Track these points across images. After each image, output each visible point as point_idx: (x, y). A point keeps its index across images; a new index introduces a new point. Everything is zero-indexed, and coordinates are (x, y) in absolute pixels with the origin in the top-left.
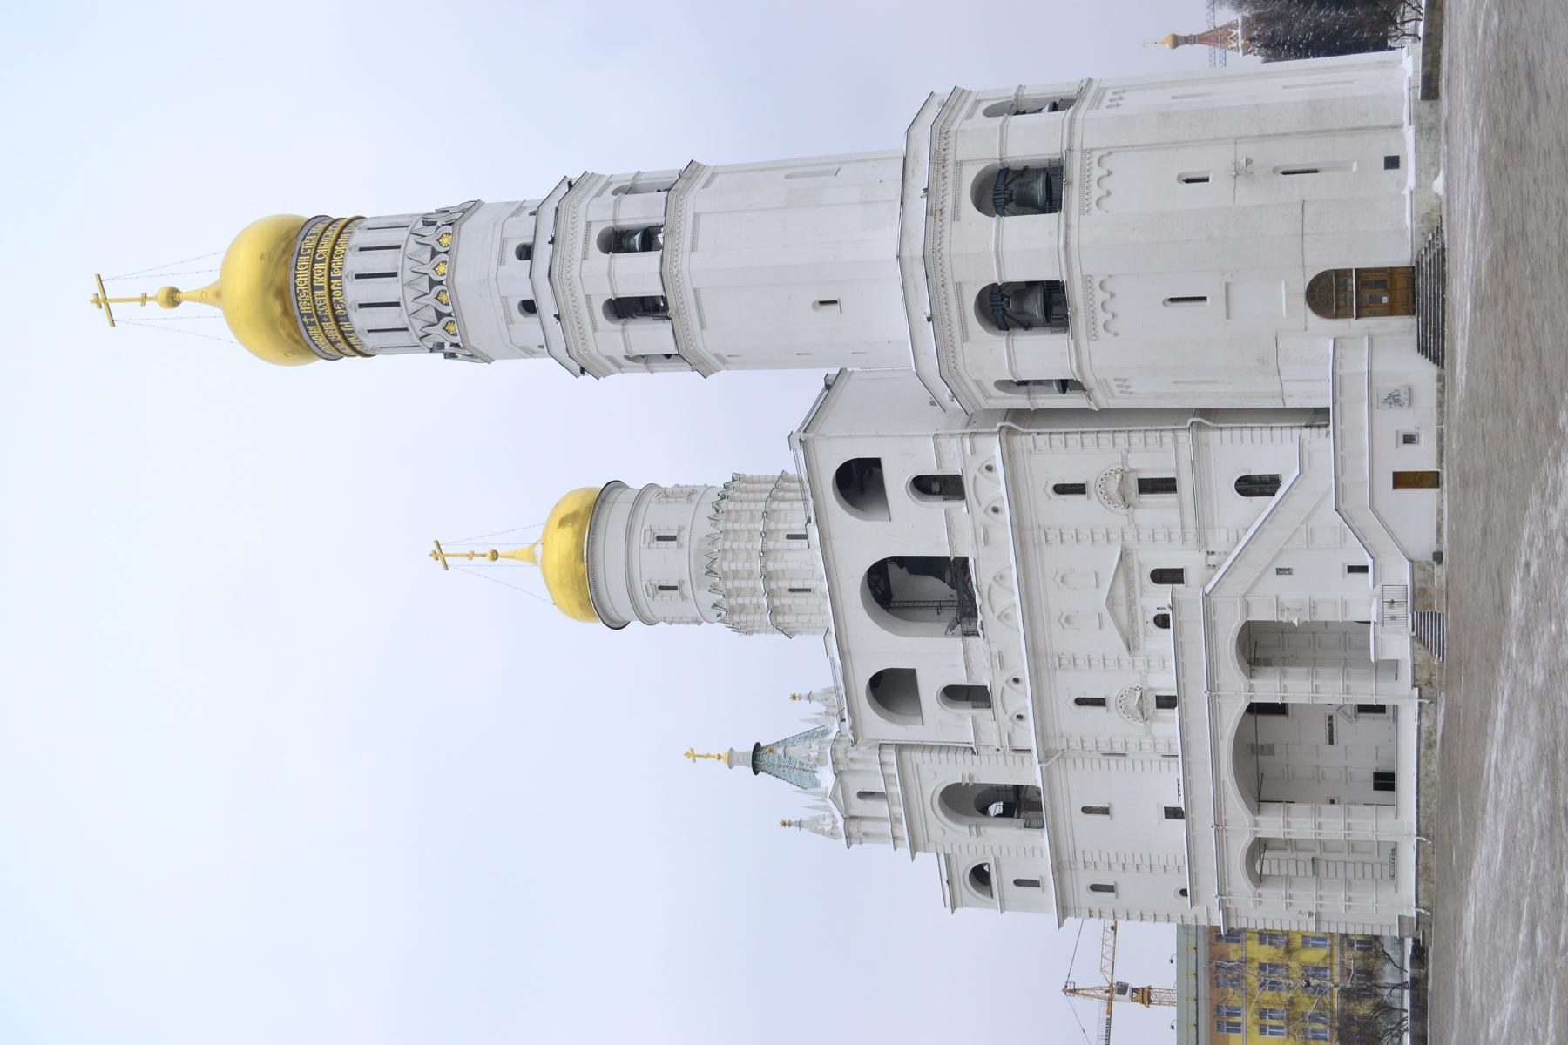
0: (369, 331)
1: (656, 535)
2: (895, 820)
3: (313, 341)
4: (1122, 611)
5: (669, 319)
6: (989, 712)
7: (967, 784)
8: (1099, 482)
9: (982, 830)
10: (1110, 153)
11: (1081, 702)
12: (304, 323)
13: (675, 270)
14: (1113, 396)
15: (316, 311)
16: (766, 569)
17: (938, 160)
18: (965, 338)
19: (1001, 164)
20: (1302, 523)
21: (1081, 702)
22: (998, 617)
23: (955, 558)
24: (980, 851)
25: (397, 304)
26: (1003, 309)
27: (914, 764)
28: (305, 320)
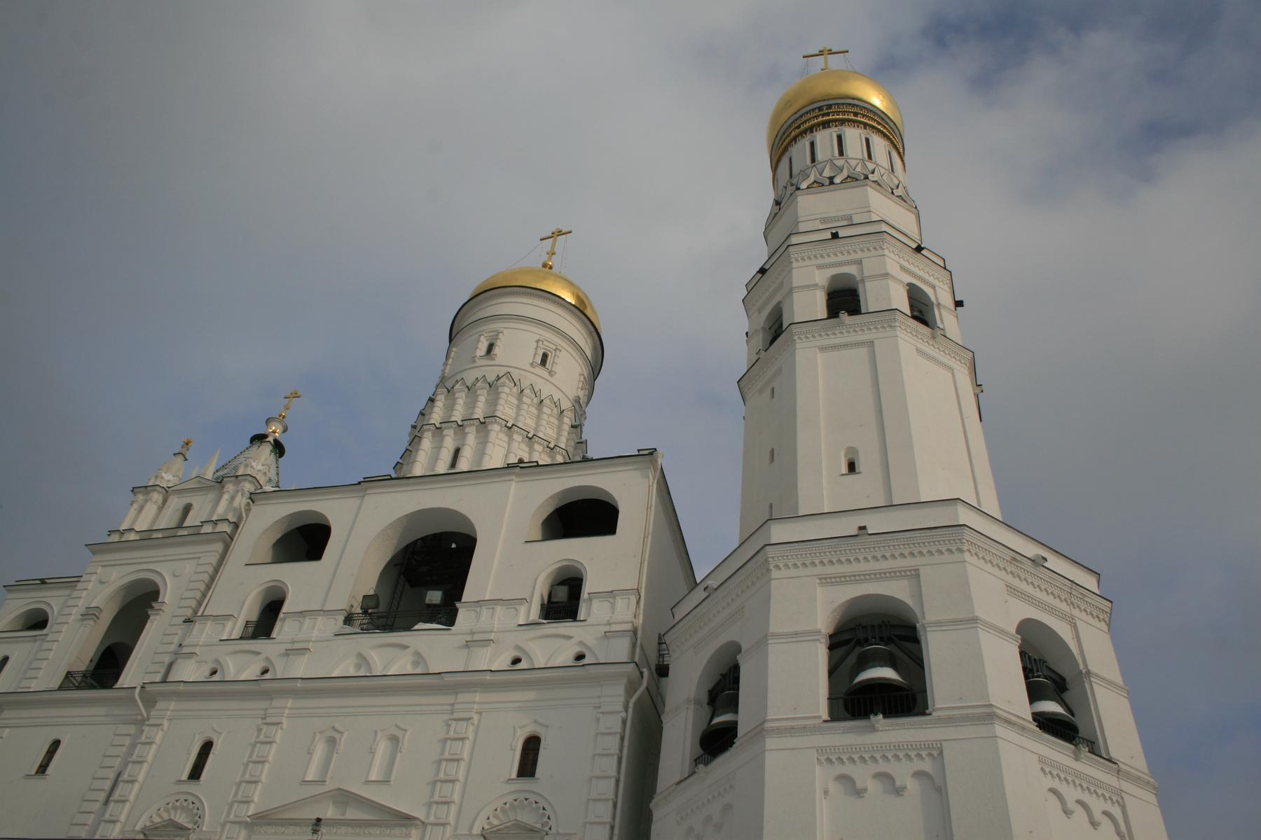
0: (812, 144)
1: (550, 354)
8: (533, 798)
9: (92, 623)
11: (207, 747)
12: (822, 106)
16: (492, 423)
18: (826, 581)
21: (207, 747)
23: (457, 610)
24: (62, 619)
25: (841, 153)
27: (200, 555)
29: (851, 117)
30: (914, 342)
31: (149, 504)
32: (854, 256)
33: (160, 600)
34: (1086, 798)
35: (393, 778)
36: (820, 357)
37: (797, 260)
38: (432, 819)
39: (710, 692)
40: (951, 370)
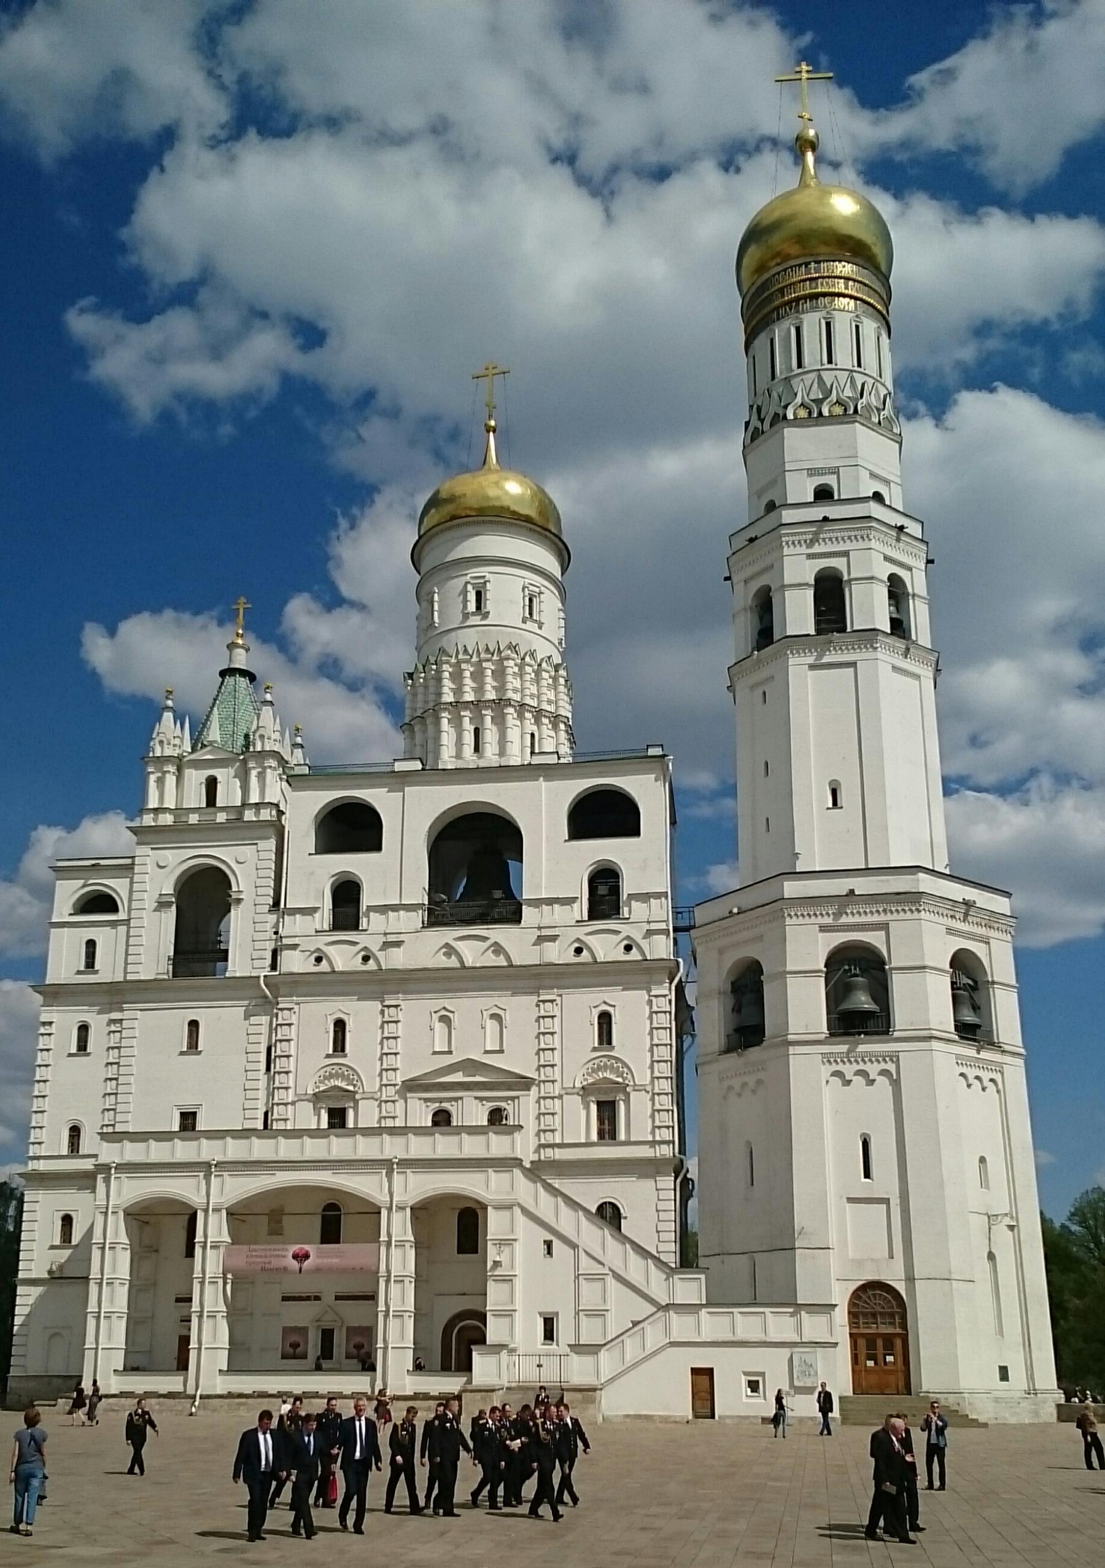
0: (798, 330)
2: (178, 811)
3: (785, 270)
4: (458, 1077)
5: (819, 631)
6: (326, 927)
7: (230, 896)
10: (998, 1091)
13: (878, 645)
14: (721, 1080)
15: (824, 277)
17: (992, 918)
18: (824, 929)
19: (988, 981)
20: (610, 1269)
22: (447, 944)
25: (830, 361)
26: (850, 969)
28: (813, 265)
29: (840, 286)
30: (889, 659)
31: (167, 775)
32: (841, 547)
33: (234, 888)
34: (980, 1073)
35: (505, 1047)
36: (810, 673)
37: (787, 543)
38: (543, 1078)
39: (733, 984)
40: (917, 677)
